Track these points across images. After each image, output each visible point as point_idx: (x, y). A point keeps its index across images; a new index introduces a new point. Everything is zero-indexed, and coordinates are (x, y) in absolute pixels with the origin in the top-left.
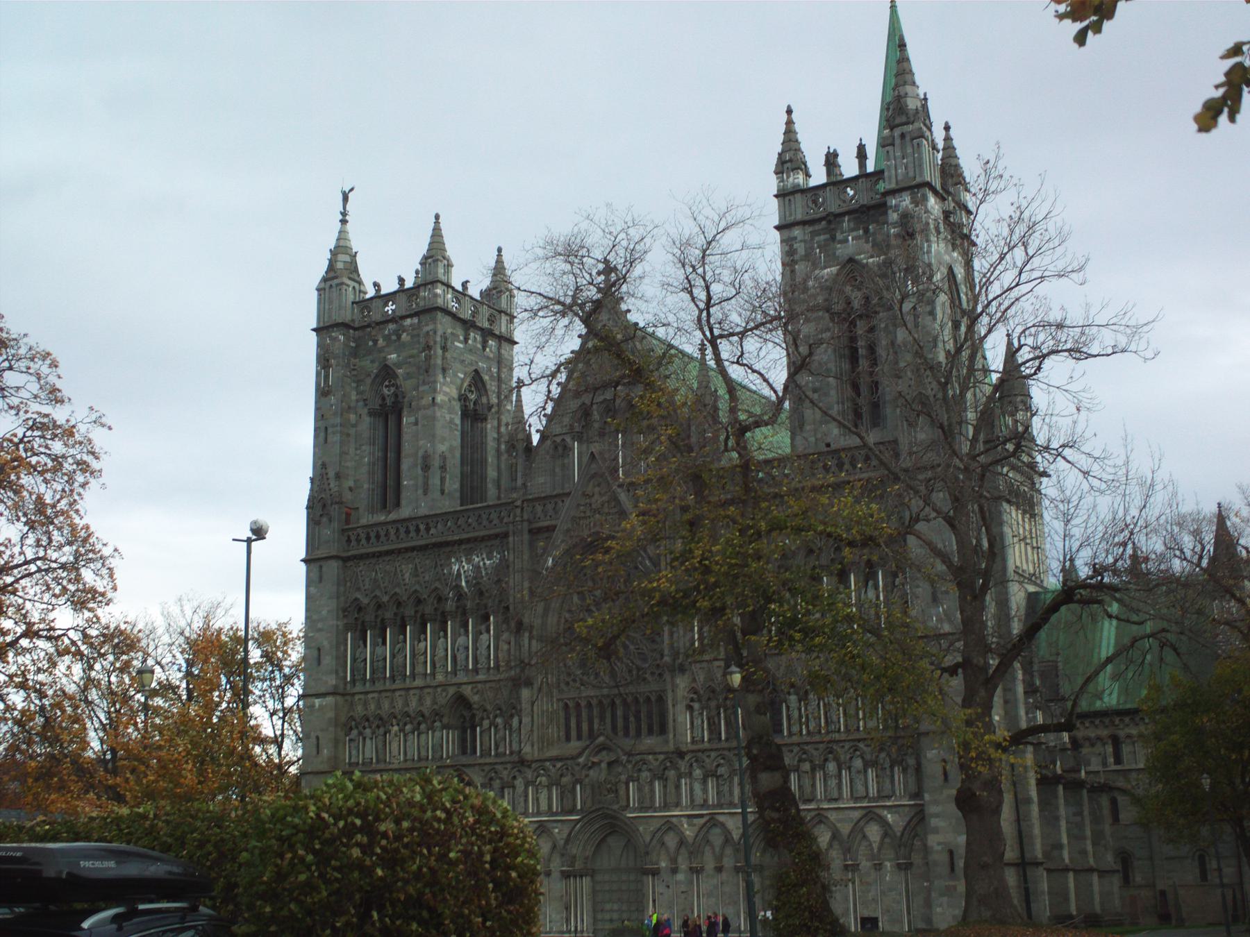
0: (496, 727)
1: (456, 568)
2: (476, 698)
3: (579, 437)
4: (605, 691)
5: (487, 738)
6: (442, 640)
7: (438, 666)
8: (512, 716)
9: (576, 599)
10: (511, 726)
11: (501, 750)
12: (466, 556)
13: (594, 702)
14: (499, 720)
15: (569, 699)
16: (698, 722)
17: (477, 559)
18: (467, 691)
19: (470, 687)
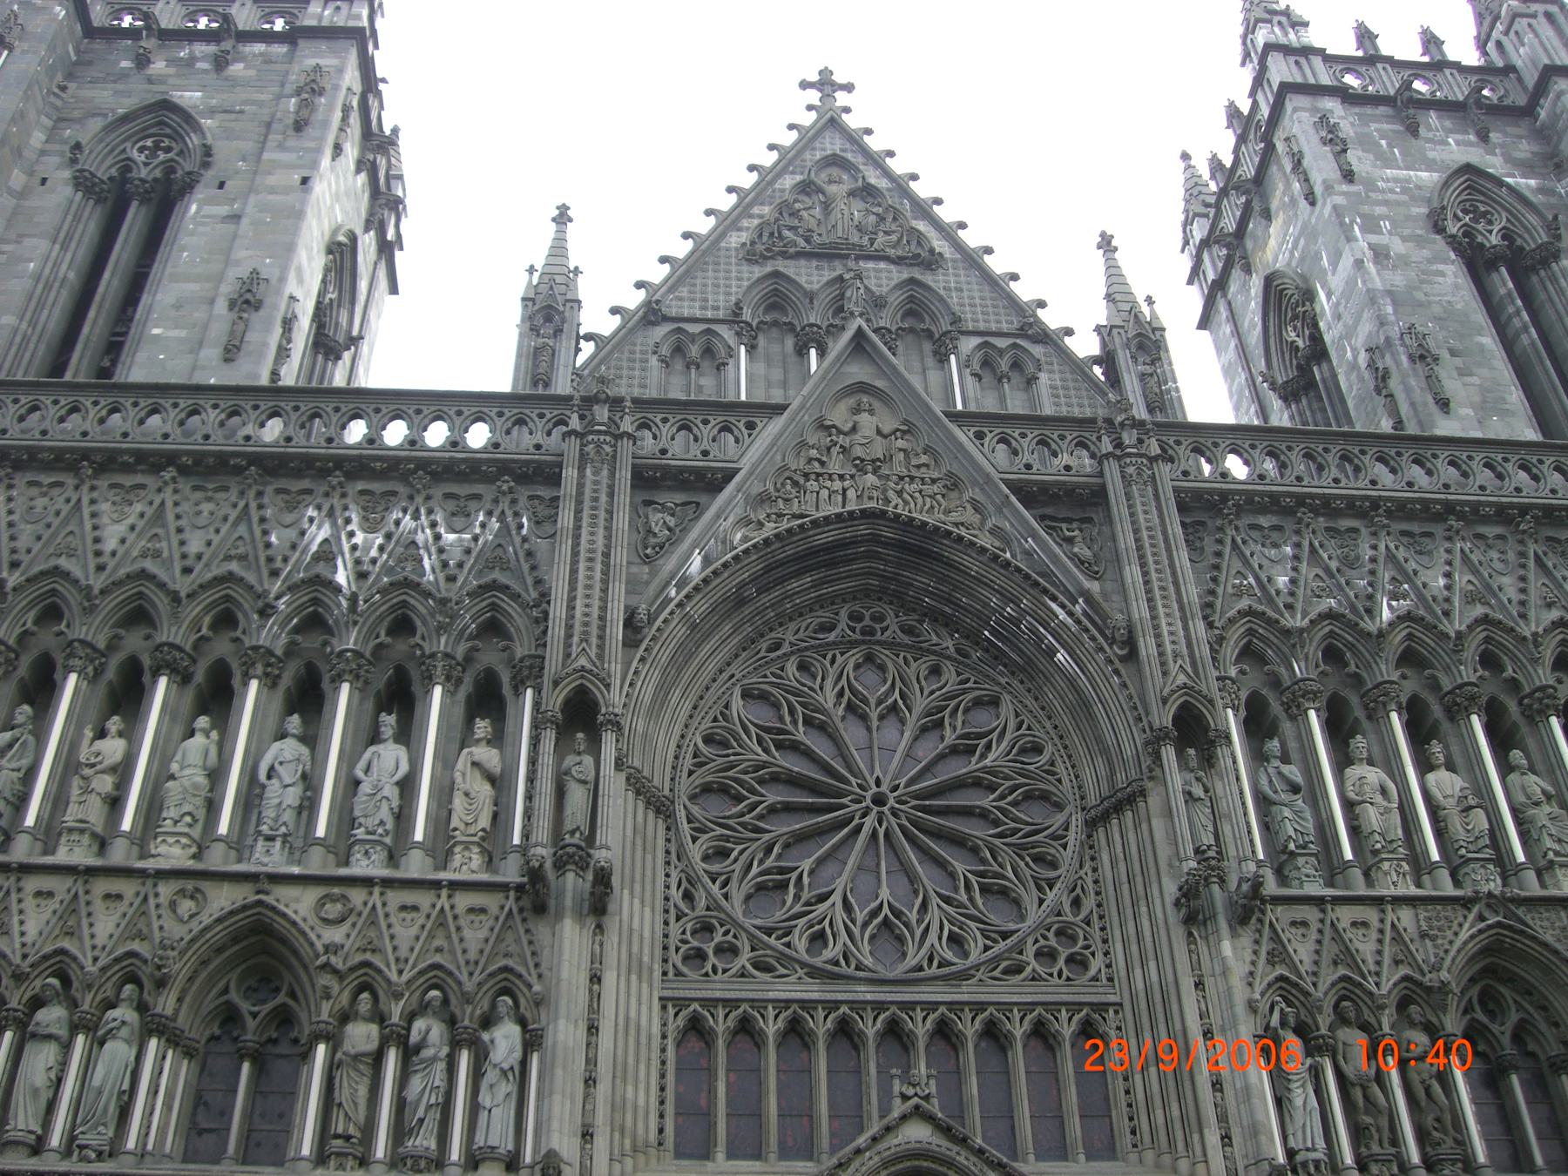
0: (409, 1054)
1: (320, 534)
2: (335, 935)
3: (750, 335)
4: (865, 993)
5: (363, 1091)
6: (199, 746)
7: (171, 813)
8: (487, 1022)
9: (737, 703)
10: (481, 1056)
11: (425, 1141)
12: (365, 509)
13: (821, 1026)
14: (429, 1030)
15: (710, 1003)
16: (1302, 1095)
17: (408, 522)
18: (299, 904)
19: (310, 896)
